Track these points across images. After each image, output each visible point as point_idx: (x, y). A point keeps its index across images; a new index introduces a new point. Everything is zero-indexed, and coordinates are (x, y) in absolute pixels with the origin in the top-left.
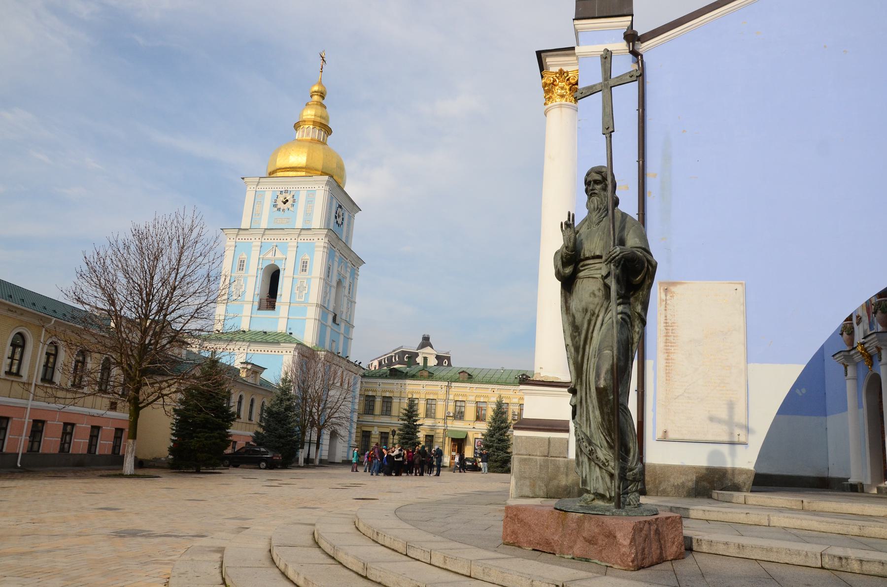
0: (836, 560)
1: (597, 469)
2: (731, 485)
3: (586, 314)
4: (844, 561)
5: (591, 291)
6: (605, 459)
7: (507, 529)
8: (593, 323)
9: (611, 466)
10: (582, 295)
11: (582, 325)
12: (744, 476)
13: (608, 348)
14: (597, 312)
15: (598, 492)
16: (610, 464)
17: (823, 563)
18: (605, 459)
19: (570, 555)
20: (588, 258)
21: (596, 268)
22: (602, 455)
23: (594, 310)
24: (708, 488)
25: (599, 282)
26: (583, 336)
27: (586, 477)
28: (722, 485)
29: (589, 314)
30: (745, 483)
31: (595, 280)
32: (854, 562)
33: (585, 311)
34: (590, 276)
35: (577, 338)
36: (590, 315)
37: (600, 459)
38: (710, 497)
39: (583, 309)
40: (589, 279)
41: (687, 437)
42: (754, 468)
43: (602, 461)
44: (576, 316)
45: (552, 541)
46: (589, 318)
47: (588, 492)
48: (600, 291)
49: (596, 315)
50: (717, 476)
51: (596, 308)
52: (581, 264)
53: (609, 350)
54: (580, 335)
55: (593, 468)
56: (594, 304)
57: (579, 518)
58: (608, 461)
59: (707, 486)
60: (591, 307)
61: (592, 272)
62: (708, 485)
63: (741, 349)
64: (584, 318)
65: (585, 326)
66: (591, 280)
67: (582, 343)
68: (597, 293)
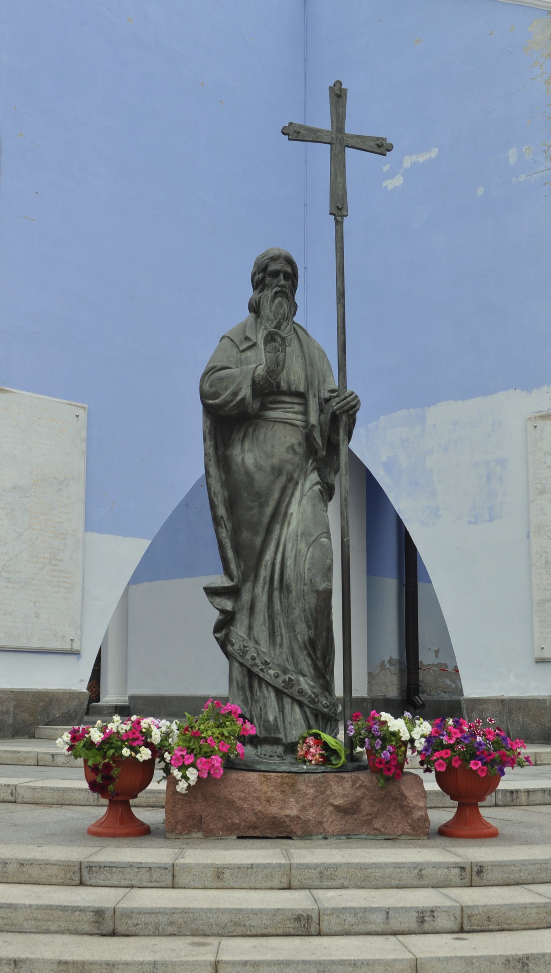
0: (508, 795)
1: (297, 709)
2: (59, 717)
4: (515, 794)
5: (289, 444)
7: (176, 812)
8: (289, 491)
10: (273, 447)
11: (269, 490)
12: (76, 702)
13: (324, 535)
14: (296, 475)
16: (320, 701)
17: (497, 800)
19: (321, 833)
20: (284, 393)
21: (296, 409)
24: (30, 722)
25: (300, 432)
26: (269, 510)
27: (275, 719)
28: (48, 718)
29: (283, 479)
30: (76, 712)
32: (523, 794)
35: (255, 511)
36: (286, 480)
37: (306, 694)
42: (88, 689)
43: (310, 696)
44: (257, 476)
45: (286, 819)
46: (283, 485)
47: (276, 741)
48: (301, 446)
49: (294, 482)
50: (42, 704)
51: (294, 471)
52: (271, 399)
53: (326, 537)
55: (287, 707)
56: (293, 464)
58: (318, 695)
59: (28, 720)
61: (290, 415)
62: (30, 718)
64: (273, 482)
65: (276, 495)
66: (288, 427)
67: (266, 520)
68: (297, 448)
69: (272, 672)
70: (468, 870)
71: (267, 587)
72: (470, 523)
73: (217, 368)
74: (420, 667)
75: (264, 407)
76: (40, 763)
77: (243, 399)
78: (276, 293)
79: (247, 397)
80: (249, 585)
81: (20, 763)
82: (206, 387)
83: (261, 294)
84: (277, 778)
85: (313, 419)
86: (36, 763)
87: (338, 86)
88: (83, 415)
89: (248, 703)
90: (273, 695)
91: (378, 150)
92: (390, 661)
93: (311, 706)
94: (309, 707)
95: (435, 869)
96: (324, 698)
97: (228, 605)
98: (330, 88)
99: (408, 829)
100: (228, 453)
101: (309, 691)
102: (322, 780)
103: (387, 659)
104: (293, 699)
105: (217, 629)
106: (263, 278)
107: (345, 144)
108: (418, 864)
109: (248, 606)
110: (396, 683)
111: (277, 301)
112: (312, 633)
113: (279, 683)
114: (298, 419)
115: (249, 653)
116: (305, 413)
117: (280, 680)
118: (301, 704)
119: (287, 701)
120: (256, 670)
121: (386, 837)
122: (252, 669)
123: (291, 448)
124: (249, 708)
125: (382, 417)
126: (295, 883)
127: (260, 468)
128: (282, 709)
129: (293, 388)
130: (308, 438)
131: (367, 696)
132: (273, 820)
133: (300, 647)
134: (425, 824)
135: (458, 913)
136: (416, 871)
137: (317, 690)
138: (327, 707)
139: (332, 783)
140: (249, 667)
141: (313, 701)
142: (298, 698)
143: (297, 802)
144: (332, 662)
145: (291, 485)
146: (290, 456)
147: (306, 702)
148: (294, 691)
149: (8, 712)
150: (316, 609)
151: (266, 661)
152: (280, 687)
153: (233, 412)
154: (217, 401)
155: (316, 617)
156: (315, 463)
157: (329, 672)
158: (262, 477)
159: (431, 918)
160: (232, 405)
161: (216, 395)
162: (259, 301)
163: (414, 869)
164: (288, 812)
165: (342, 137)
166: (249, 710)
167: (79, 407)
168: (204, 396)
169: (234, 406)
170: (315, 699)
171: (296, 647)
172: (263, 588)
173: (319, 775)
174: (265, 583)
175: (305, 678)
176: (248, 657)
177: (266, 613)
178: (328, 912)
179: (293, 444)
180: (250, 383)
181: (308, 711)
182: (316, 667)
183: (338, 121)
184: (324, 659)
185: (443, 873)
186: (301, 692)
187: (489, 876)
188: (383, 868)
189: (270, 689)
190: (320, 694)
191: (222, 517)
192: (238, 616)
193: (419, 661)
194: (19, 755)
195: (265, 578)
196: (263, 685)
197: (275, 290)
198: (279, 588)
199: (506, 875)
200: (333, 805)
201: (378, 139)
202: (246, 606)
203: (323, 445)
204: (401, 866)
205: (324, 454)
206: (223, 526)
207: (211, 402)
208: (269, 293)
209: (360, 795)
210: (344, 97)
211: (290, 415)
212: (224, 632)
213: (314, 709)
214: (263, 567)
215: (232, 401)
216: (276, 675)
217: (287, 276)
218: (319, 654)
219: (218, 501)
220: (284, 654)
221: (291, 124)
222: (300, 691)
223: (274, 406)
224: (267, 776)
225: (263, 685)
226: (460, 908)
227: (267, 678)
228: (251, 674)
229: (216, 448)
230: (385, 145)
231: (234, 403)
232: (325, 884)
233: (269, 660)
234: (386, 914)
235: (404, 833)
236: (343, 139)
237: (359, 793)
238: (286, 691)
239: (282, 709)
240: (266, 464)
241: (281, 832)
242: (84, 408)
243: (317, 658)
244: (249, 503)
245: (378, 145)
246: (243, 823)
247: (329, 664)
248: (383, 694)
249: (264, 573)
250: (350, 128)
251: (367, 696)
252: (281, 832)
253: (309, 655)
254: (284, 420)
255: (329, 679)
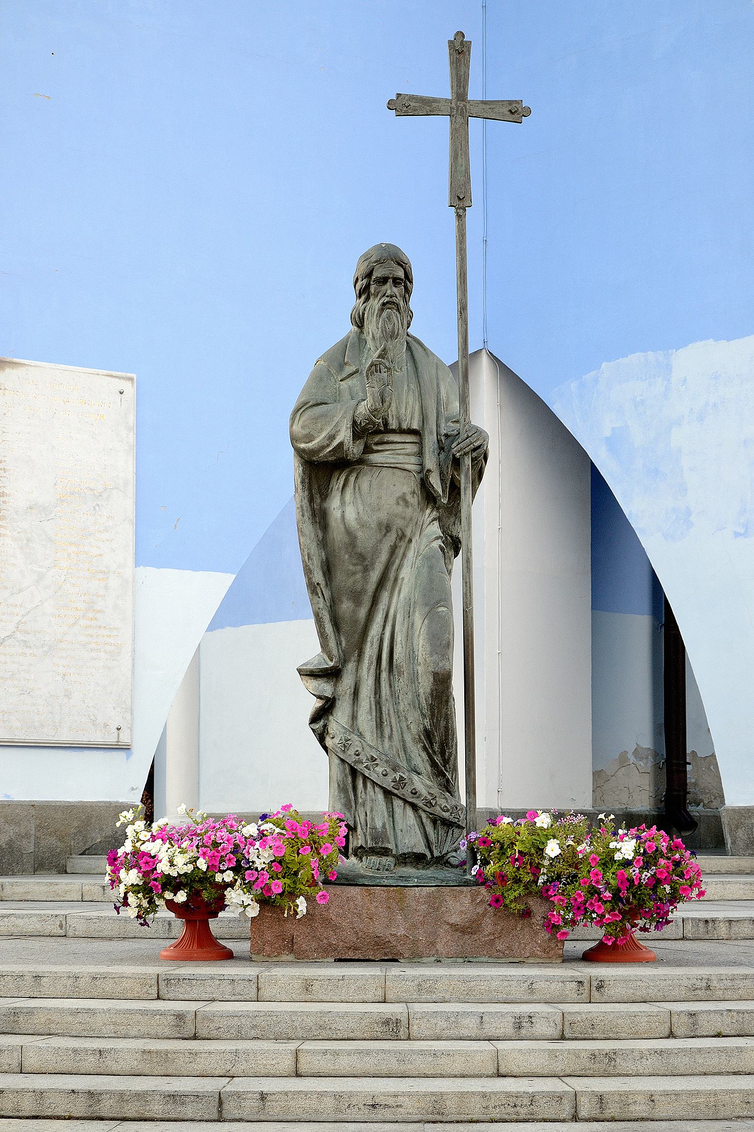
1: (410, 812)
3: (385, 535)
5: (399, 494)
6: (429, 793)
9: (440, 806)
11: (376, 551)
14: (408, 533)
15: (415, 851)
16: (438, 803)
18: (429, 793)
19: (433, 956)
20: (393, 431)
21: (408, 451)
22: (422, 786)
23: (403, 528)
25: (413, 478)
26: (375, 576)
29: (392, 537)
31: (405, 473)
33: (383, 528)
34: (397, 465)
35: (359, 576)
38: (63, 871)
39: (380, 525)
40: (395, 470)
41: (21, 736)
43: (425, 799)
44: (360, 534)
45: (392, 939)
47: (385, 852)
52: (377, 439)
54: (366, 570)
57: (429, 895)
60: (399, 522)
61: (401, 459)
63: (127, 533)
64: (381, 541)
65: (384, 557)
68: (409, 498)
69: (379, 769)
70: (586, 985)
71: (373, 667)
72: (737, 535)
73: (311, 403)
74: (688, 761)
75: (368, 450)
76: (86, 898)
77: (341, 444)
78: (384, 304)
79: (346, 441)
80: (351, 666)
81: (59, 899)
82: (297, 428)
83: (365, 305)
84: (382, 892)
85: (430, 462)
86: (80, 899)
87: (459, 39)
88: (130, 389)
89: (351, 807)
90: (380, 796)
91: (511, 117)
92: (636, 753)
93: (427, 809)
94: (425, 811)
95: (548, 983)
96: (443, 800)
97: (327, 689)
98: (450, 42)
99: (538, 951)
100: (325, 505)
101: (424, 791)
102: (436, 895)
103: (631, 749)
104: (405, 801)
105: (314, 720)
106: (368, 286)
107: (468, 114)
108: (529, 977)
109: (350, 691)
110: (647, 788)
111: (384, 314)
112: (427, 722)
113: (388, 784)
114: (411, 463)
115: (351, 748)
116: (420, 454)
117: (389, 779)
118: (414, 807)
119: (398, 803)
120: (359, 767)
121: (511, 960)
122: (355, 767)
123: (403, 499)
124: (353, 812)
125: (604, 364)
126: (390, 996)
127: (363, 525)
128: (392, 814)
129: (405, 426)
130: (424, 485)
131: (591, 809)
132: (376, 939)
133: (414, 739)
134: (557, 945)
135: (559, 1019)
136: (526, 985)
137: (436, 791)
138: (448, 811)
139: (448, 898)
140: (352, 765)
141: (429, 804)
142: (410, 800)
143: (406, 918)
144: (453, 757)
145: (403, 544)
146: (400, 509)
147: (421, 804)
148: (406, 792)
149: (27, 836)
150: (432, 694)
151: (372, 757)
152: (390, 788)
153: (330, 459)
154: (310, 445)
155: (432, 703)
156: (435, 513)
157: (450, 768)
158: (366, 535)
159: (529, 1024)
160: (328, 450)
161: (309, 438)
162: (363, 314)
163: (524, 983)
164: (393, 931)
165: (465, 106)
166: (353, 817)
167: (123, 378)
168: (294, 439)
169: (330, 452)
170: (431, 801)
171: (408, 739)
172: (369, 669)
173: (433, 889)
174: (371, 664)
175: (419, 776)
176: (351, 752)
177: (372, 699)
178: (419, 1016)
179: (404, 494)
180: (350, 424)
181: (423, 815)
182: (434, 764)
183: (459, 86)
184: (443, 753)
185: (558, 987)
186: (414, 793)
187: (608, 991)
188: (488, 981)
189: (377, 789)
190: (438, 796)
191: (318, 584)
192: (338, 704)
193: (688, 751)
194: (56, 887)
195: (370, 656)
196: (369, 785)
197: (381, 301)
198: (387, 670)
199: (632, 991)
200: (448, 924)
201: (511, 102)
202: (348, 691)
203: (443, 491)
204: (509, 978)
205: (445, 502)
206: (320, 595)
207: (302, 446)
208: (375, 303)
209: (481, 912)
210: (467, 53)
211: (401, 459)
212: (322, 723)
213: (431, 814)
214: (369, 644)
215: (328, 445)
216: (384, 773)
217: (396, 281)
218: (436, 747)
219: (313, 564)
220: (394, 748)
221: (399, 95)
222: (413, 791)
223: (379, 448)
224: (370, 890)
225: (369, 785)
226: (561, 1014)
227: (374, 777)
228: (354, 772)
229: (311, 500)
230: (520, 109)
231: (330, 448)
232: (424, 997)
233: (376, 755)
234: (480, 1019)
235: (533, 955)
236: (466, 109)
237: (480, 910)
238: (396, 791)
239: (392, 814)
240: (372, 520)
241: (386, 954)
242: (131, 379)
243: (434, 752)
244: (351, 567)
245: (510, 111)
246: (341, 943)
247: (449, 759)
248: (624, 807)
249: (370, 651)
250: (474, 93)
251: (591, 809)
252: (386, 954)
253: (425, 749)
254: (392, 466)
255: (450, 778)
